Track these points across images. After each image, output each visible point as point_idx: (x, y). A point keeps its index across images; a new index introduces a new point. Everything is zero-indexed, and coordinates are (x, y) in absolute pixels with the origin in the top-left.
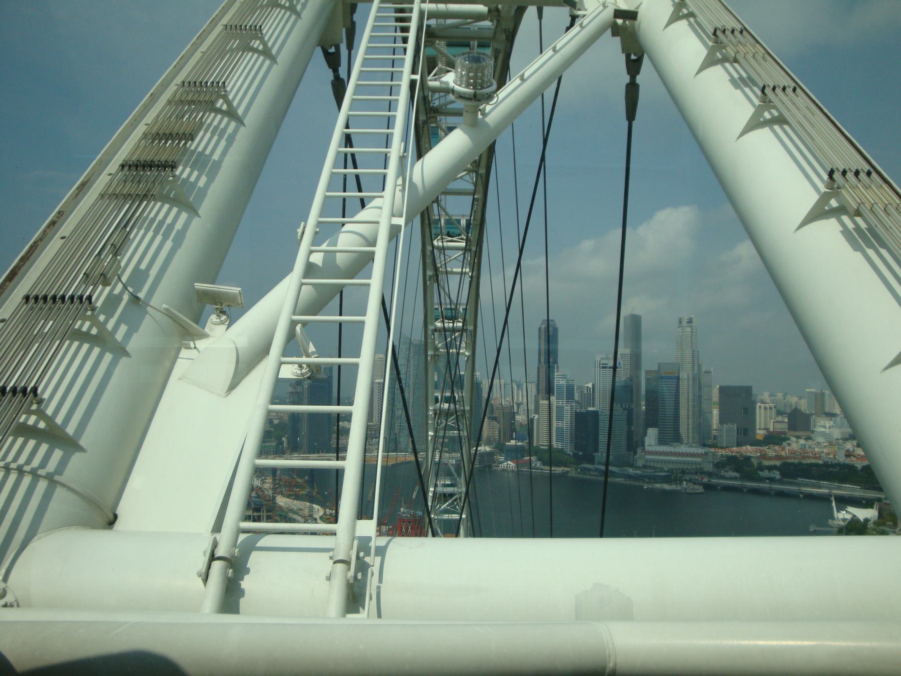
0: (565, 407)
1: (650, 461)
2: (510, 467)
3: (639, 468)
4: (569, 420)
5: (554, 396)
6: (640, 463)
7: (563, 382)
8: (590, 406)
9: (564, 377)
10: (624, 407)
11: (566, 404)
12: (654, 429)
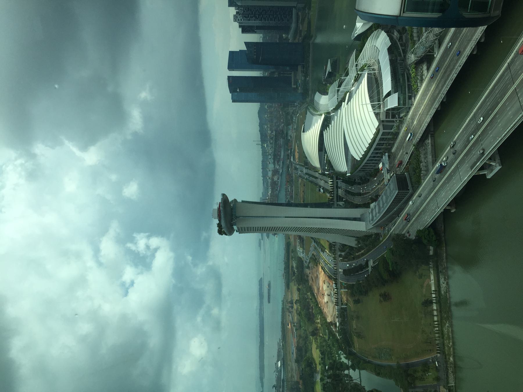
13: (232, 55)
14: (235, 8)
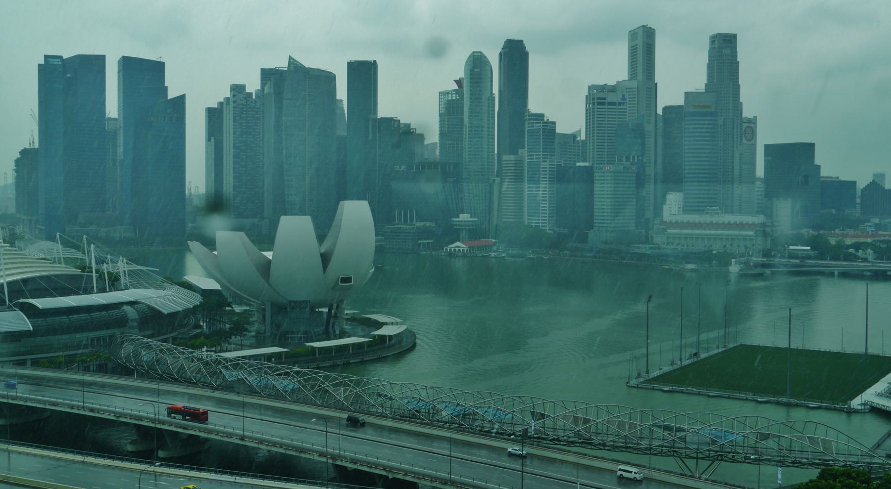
0: (541, 163)
2: (459, 250)
4: (547, 176)
5: (523, 147)
7: (539, 126)
8: (579, 162)
10: (631, 160)
11: (543, 158)
13: (158, 68)
14: (258, 90)
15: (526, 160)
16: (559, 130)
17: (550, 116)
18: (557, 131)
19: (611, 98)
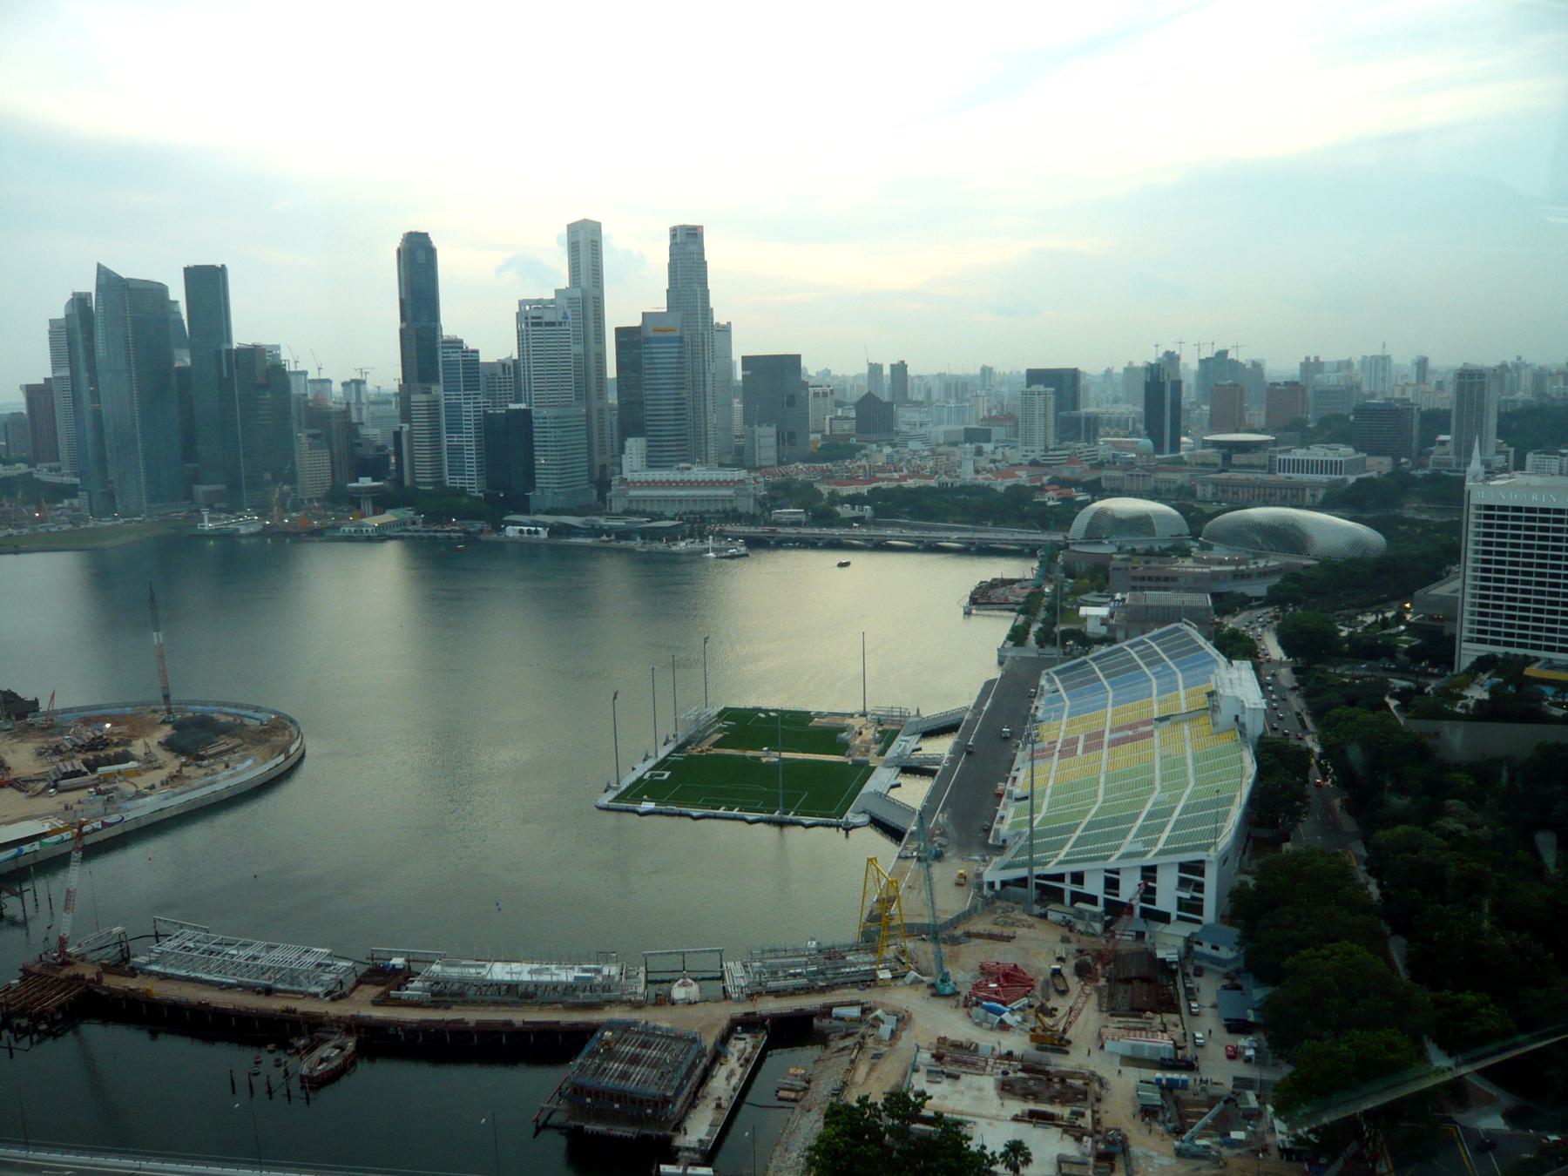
1: (638, 500)
3: (618, 516)
6: (618, 506)
9: (456, 344)
12: (639, 439)
15: (443, 402)
16: (483, 358)
17: (470, 344)
18: (482, 360)
19: (549, 317)
